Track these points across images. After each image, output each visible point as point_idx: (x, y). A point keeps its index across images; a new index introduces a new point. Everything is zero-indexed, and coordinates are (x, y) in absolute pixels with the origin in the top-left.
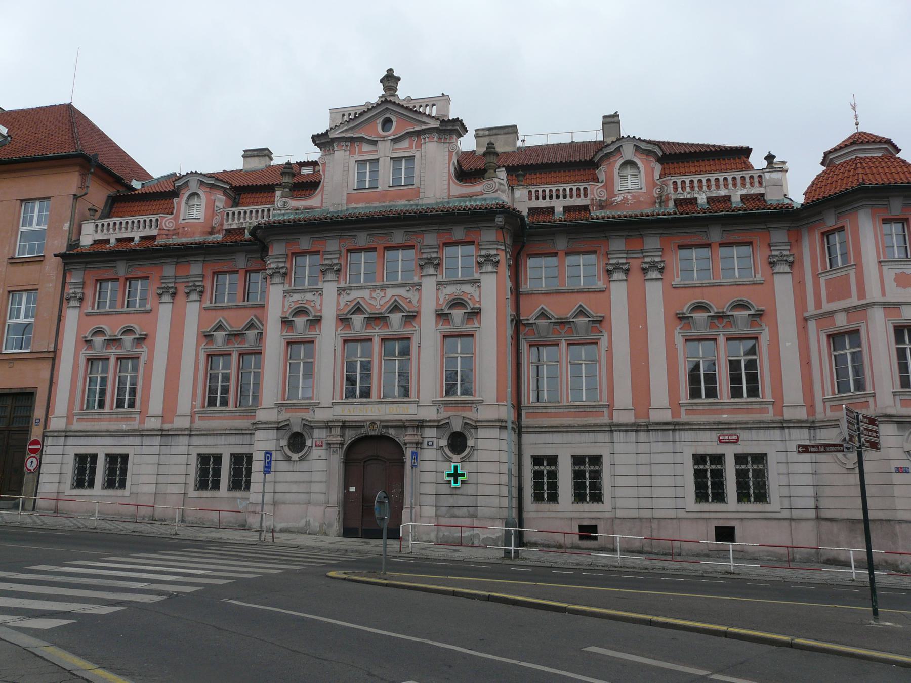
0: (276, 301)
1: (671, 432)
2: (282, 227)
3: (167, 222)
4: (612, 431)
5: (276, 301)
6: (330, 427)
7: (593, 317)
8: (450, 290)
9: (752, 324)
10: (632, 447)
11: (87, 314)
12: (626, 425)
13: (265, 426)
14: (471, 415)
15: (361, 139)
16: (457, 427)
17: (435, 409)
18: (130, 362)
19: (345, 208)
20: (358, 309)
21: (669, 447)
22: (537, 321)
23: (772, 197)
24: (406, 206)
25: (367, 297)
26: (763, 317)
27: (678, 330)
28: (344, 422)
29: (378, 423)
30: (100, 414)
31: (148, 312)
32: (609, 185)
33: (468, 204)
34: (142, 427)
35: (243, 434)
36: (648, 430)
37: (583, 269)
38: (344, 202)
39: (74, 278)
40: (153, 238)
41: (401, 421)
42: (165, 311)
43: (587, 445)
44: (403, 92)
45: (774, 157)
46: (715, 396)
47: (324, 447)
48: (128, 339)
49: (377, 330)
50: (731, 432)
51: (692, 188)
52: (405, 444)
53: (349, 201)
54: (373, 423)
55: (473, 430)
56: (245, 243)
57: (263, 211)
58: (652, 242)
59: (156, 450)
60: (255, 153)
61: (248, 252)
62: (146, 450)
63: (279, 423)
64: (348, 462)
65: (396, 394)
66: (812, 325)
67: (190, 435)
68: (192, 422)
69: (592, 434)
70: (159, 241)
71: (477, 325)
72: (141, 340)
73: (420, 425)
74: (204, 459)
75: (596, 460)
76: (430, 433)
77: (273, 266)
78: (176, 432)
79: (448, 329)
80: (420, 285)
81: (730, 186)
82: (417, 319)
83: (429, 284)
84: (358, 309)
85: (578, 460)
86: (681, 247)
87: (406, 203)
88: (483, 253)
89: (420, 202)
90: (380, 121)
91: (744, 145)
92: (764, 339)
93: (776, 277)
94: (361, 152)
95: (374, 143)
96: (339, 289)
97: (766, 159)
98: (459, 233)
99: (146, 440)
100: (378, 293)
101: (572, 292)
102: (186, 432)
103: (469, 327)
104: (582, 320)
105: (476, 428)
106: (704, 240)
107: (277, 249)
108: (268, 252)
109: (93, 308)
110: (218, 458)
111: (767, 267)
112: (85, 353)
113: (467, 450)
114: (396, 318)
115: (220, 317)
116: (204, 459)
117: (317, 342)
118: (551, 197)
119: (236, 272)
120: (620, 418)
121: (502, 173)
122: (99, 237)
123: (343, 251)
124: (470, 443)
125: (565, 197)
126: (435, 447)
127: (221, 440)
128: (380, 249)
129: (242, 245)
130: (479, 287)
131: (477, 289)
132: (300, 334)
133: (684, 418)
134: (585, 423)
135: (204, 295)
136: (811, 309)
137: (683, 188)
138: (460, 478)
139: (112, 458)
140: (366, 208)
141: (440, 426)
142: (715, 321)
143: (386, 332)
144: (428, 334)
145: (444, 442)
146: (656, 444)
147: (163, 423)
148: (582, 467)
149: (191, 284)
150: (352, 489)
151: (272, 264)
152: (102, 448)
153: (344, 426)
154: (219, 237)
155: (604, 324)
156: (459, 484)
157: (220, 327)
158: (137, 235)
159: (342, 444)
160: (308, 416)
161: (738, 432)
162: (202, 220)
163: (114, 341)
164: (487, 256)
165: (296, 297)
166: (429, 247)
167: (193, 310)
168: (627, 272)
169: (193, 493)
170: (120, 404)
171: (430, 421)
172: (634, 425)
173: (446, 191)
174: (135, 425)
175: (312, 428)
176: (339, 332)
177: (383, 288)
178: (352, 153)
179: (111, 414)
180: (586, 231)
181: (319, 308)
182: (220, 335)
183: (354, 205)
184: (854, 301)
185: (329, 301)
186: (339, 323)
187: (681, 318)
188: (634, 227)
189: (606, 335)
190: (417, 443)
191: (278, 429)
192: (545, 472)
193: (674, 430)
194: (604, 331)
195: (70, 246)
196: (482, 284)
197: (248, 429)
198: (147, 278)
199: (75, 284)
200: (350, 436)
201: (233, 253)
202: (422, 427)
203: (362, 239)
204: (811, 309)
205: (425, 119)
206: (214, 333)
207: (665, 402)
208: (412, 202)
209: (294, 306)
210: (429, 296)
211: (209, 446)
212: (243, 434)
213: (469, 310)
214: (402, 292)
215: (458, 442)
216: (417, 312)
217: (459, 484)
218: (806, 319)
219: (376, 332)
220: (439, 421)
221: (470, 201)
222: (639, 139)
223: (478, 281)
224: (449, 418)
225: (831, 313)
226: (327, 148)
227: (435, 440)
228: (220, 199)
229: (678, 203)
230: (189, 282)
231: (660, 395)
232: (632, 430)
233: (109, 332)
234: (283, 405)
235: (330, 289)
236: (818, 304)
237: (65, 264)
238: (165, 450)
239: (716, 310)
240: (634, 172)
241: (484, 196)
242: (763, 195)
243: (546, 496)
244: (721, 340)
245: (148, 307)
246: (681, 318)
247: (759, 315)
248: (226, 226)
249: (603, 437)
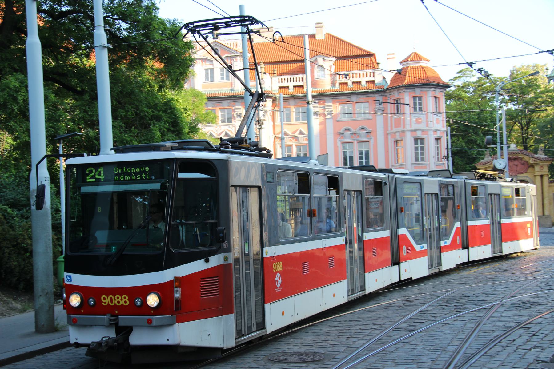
9: (367, 136)
66: (389, 136)
92: (372, 141)
93: (378, 117)
94: (206, 65)
136: (389, 131)
142: (353, 135)
184: (401, 129)
204: (389, 131)
218: (387, 134)
225: (395, 133)
236: (392, 129)
244: (355, 143)
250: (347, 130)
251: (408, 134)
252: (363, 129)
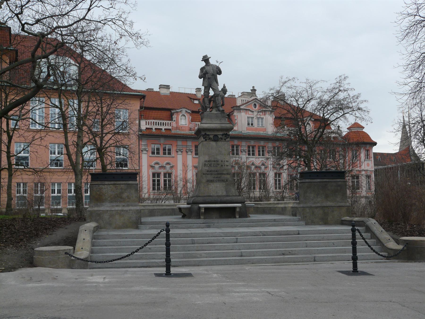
15: (249, 110)
39: (143, 143)
40: (170, 129)
42: (180, 157)
48: (168, 167)
72: (172, 167)
84: (253, 164)
90: (253, 104)
94: (248, 114)
95: (253, 112)
100: (257, 160)
112: (151, 171)
114: (263, 167)
162: (187, 125)
163: (162, 167)
177: (258, 158)
178: (246, 114)
183: (248, 131)
199: (144, 145)
251: (363, 173)
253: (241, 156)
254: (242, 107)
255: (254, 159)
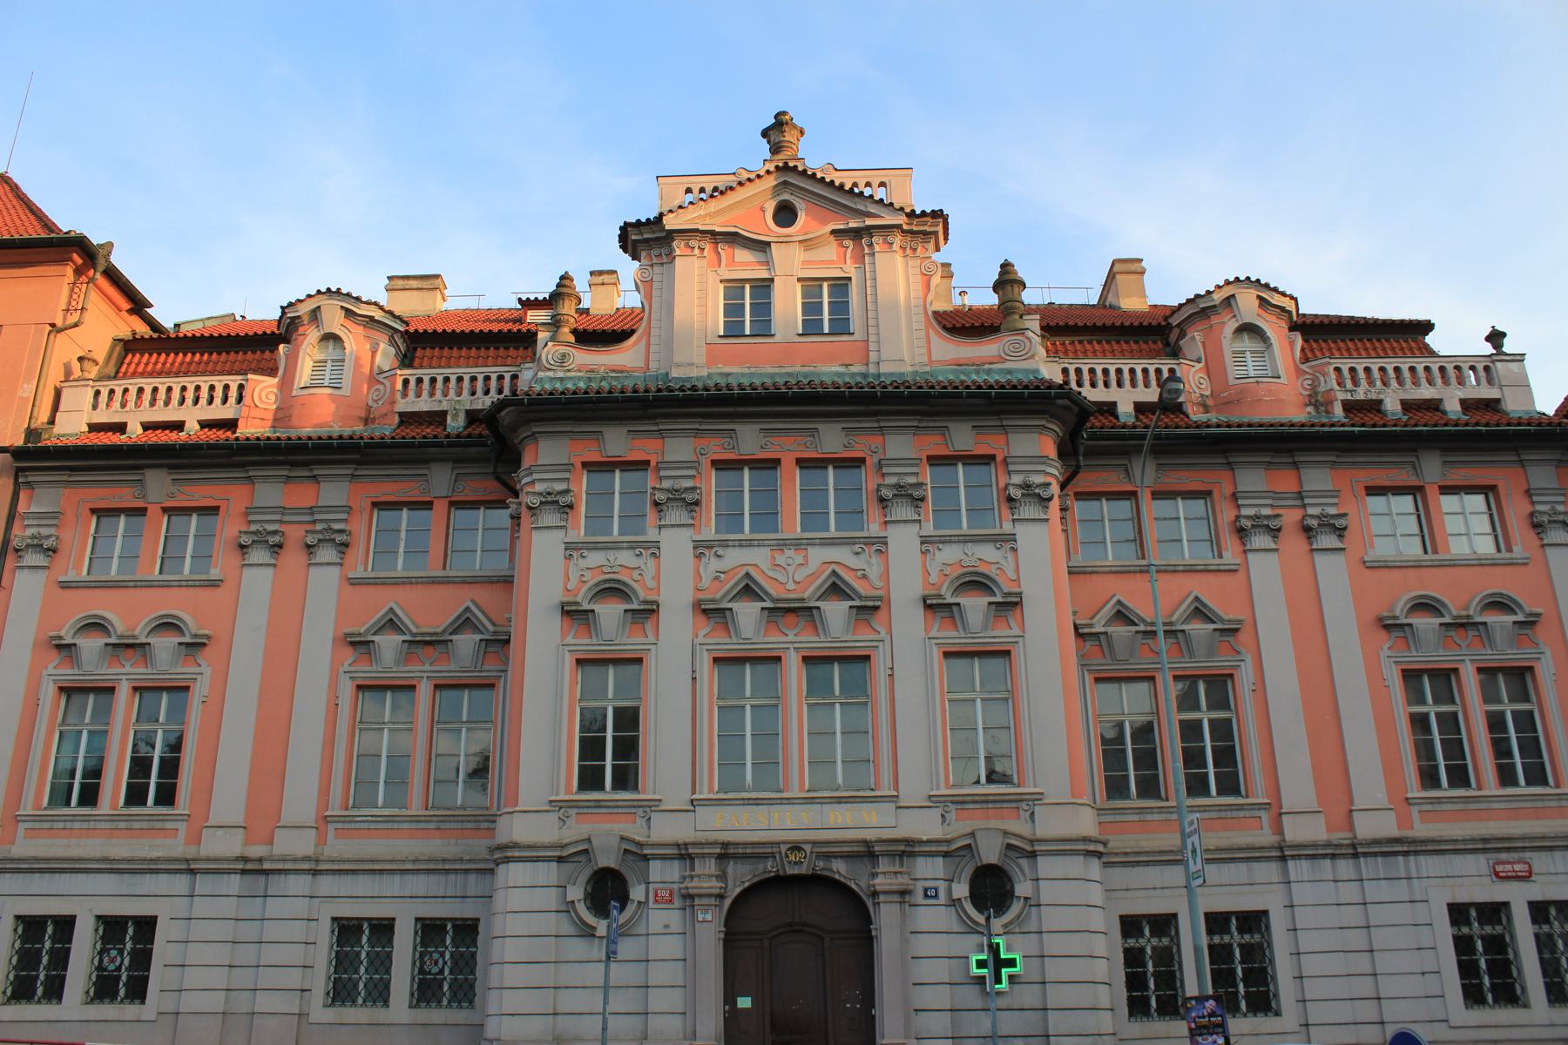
0: (550, 566)
1: (1401, 858)
2: (569, 402)
3: (264, 389)
4: (1283, 858)
5: (550, 566)
6: (691, 857)
7: (1222, 621)
8: (950, 554)
10: (1327, 892)
11: (65, 586)
12: (1315, 845)
13: (531, 854)
14: (1019, 826)
16: (990, 853)
17: (937, 813)
18: (165, 697)
19: (704, 373)
20: (749, 590)
21: (1400, 890)
22: (1110, 629)
23: (1513, 406)
24: (840, 375)
25: (765, 565)
26: (1539, 628)
27: (1385, 652)
28: (725, 845)
29: (808, 848)
30: (85, 818)
31: (214, 584)
32: (1213, 368)
33: (974, 377)
34: (191, 852)
35: (447, 871)
36: (1355, 856)
37: (1179, 528)
38: (703, 360)
40: (231, 424)
41: (865, 842)
42: (257, 583)
43: (1231, 890)
44: (812, 154)
45: (1503, 335)
46: (1467, 784)
47: (677, 903)
48: (164, 645)
49: (791, 638)
50: (1515, 856)
51: (1371, 383)
52: (875, 894)
53: (712, 358)
54: (796, 847)
55: (1024, 862)
56: (457, 441)
57: (487, 378)
58: (1317, 478)
59: (228, 907)
60: (414, 284)
61: (457, 461)
62: (201, 907)
63: (563, 847)
64: (732, 939)
65: (840, 780)
67: (315, 873)
68: (321, 840)
69: (1243, 866)
70: (246, 430)
71: (1016, 631)
72: (196, 646)
73: (906, 850)
74: (346, 929)
75: (1254, 921)
76: (929, 869)
77: (539, 487)
78: (280, 866)
79: (954, 637)
80: (883, 541)
81: (1439, 381)
82: (881, 614)
83: (903, 540)
84: (749, 590)
85: (1216, 922)
86: (1373, 491)
87: (841, 369)
88: (1017, 479)
89: (872, 369)
91: (1421, 317)
95: (762, 246)
96: (698, 545)
97: (1488, 339)
98: (963, 437)
99: (203, 884)
101: (1172, 570)
102: (306, 866)
103: (1000, 634)
104: (1198, 628)
105: (1033, 855)
106: (1412, 481)
107: (548, 458)
108: (516, 462)
109: (79, 573)
110: (383, 929)
111: (1531, 534)
113: (631, 908)
115: (390, 600)
116: (346, 929)
117: (651, 663)
118: (1106, 385)
119: (428, 505)
120: (1298, 831)
121: (1033, 324)
122: (102, 417)
123: (705, 462)
124: (1022, 889)
125: (1134, 384)
126: (942, 899)
127: (393, 885)
128: (788, 461)
129: (450, 445)
130: (1014, 550)
131: (1010, 555)
132: (610, 642)
133: (1421, 830)
134: (1224, 843)
135: (350, 552)
137: (1355, 383)
138: (1005, 971)
139: (112, 927)
140: (743, 375)
141: (951, 852)
142: (1452, 633)
143: (813, 642)
144: (908, 648)
145: (962, 890)
146: (1383, 886)
147: (247, 843)
148: (1226, 939)
149: (319, 527)
150: (744, 1002)
151: (534, 486)
152: (87, 901)
153: (727, 853)
154: (386, 429)
155: (1245, 636)
156: (1004, 985)
157: (391, 624)
158: (192, 415)
159: (721, 897)
160: (636, 831)
161: (1527, 855)
164: (1026, 486)
165: (595, 559)
166: (898, 462)
167: (324, 584)
168: (1275, 532)
169: (321, 1013)
170: (136, 796)
171: (929, 842)
172: (1328, 845)
173: (924, 350)
174: (176, 846)
175: (646, 858)
176: (700, 639)
177: (798, 544)
179: (114, 818)
180: (1190, 446)
181: (651, 584)
182: (389, 643)
185: (676, 569)
186: (701, 618)
187: (1389, 626)
188: (1281, 444)
189: (1249, 659)
190: (903, 893)
191: (560, 860)
192: (1149, 951)
193: (1406, 854)
194: (1243, 651)
195: (32, 433)
196: (1020, 545)
197: (461, 860)
198: (213, 510)
199: (39, 516)
200: (740, 877)
201: (425, 462)
202: (912, 854)
203: (750, 439)
205: (872, 209)
206: (376, 638)
207: (1381, 797)
208: (853, 369)
209: (592, 579)
210: (907, 564)
211: (363, 899)
212: (447, 871)
213: (999, 599)
214: (842, 555)
215: (992, 889)
216: (880, 598)
217: (1004, 985)
219: (793, 641)
220: (949, 842)
221: (977, 372)
222: (1267, 286)
223: (1011, 538)
224: (972, 834)
226: (654, 252)
227: (942, 886)
228: (385, 355)
229: (1349, 407)
230: (314, 522)
231: (1369, 785)
232: (1325, 856)
233: (119, 626)
234: (571, 804)
235: (676, 543)
237: (18, 472)
238: (253, 907)
239: (1455, 613)
240: (1259, 346)
241: (1008, 365)
242: (1498, 401)
243: (1153, 1003)
245: (215, 573)
246: (1389, 626)
247: (1530, 623)
248: (403, 405)
249: (1268, 871)
250: (1425, 606)
252: (1499, 604)
253: (652, 534)
254: (670, 223)
255: (757, 559)
